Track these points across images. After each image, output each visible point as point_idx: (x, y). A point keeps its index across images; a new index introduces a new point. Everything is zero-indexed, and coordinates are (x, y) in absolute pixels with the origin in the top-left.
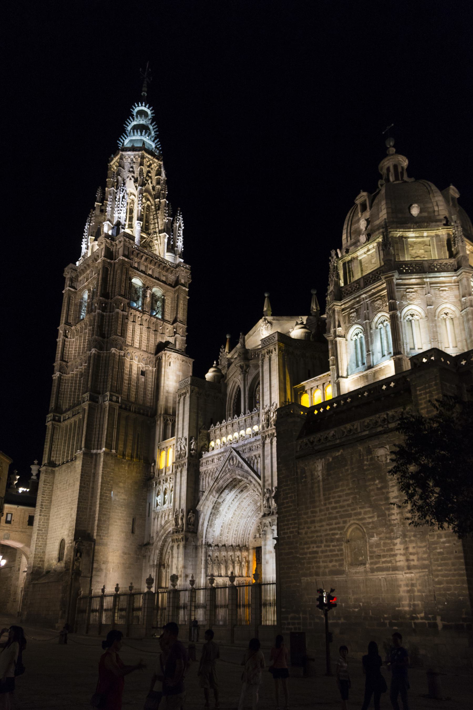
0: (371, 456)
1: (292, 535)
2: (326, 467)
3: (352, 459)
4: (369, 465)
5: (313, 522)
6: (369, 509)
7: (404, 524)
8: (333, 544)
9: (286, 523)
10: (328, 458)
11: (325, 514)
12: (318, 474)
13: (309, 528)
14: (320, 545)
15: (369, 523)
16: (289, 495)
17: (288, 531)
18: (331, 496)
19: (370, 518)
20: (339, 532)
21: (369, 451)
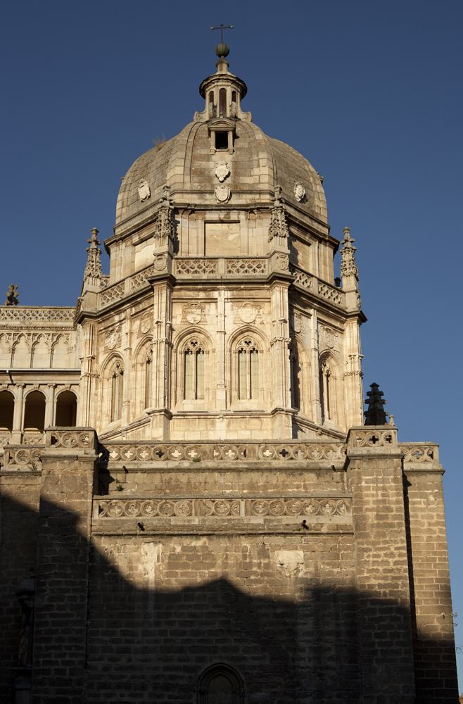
0: (266, 561)
1: (68, 668)
2: (167, 561)
3: (227, 558)
4: (262, 575)
5: (127, 650)
6: (256, 645)
7: (320, 675)
8: (171, 693)
9: (53, 643)
10: (172, 545)
11: (156, 641)
12: (145, 569)
13: (111, 659)
14: (138, 692)
15: (254, 667)
16: (67, 595)
17: (59, 660)
18: (173, 611)
19: (254, 658)
20: (187, 675)
21: (264, 553)
